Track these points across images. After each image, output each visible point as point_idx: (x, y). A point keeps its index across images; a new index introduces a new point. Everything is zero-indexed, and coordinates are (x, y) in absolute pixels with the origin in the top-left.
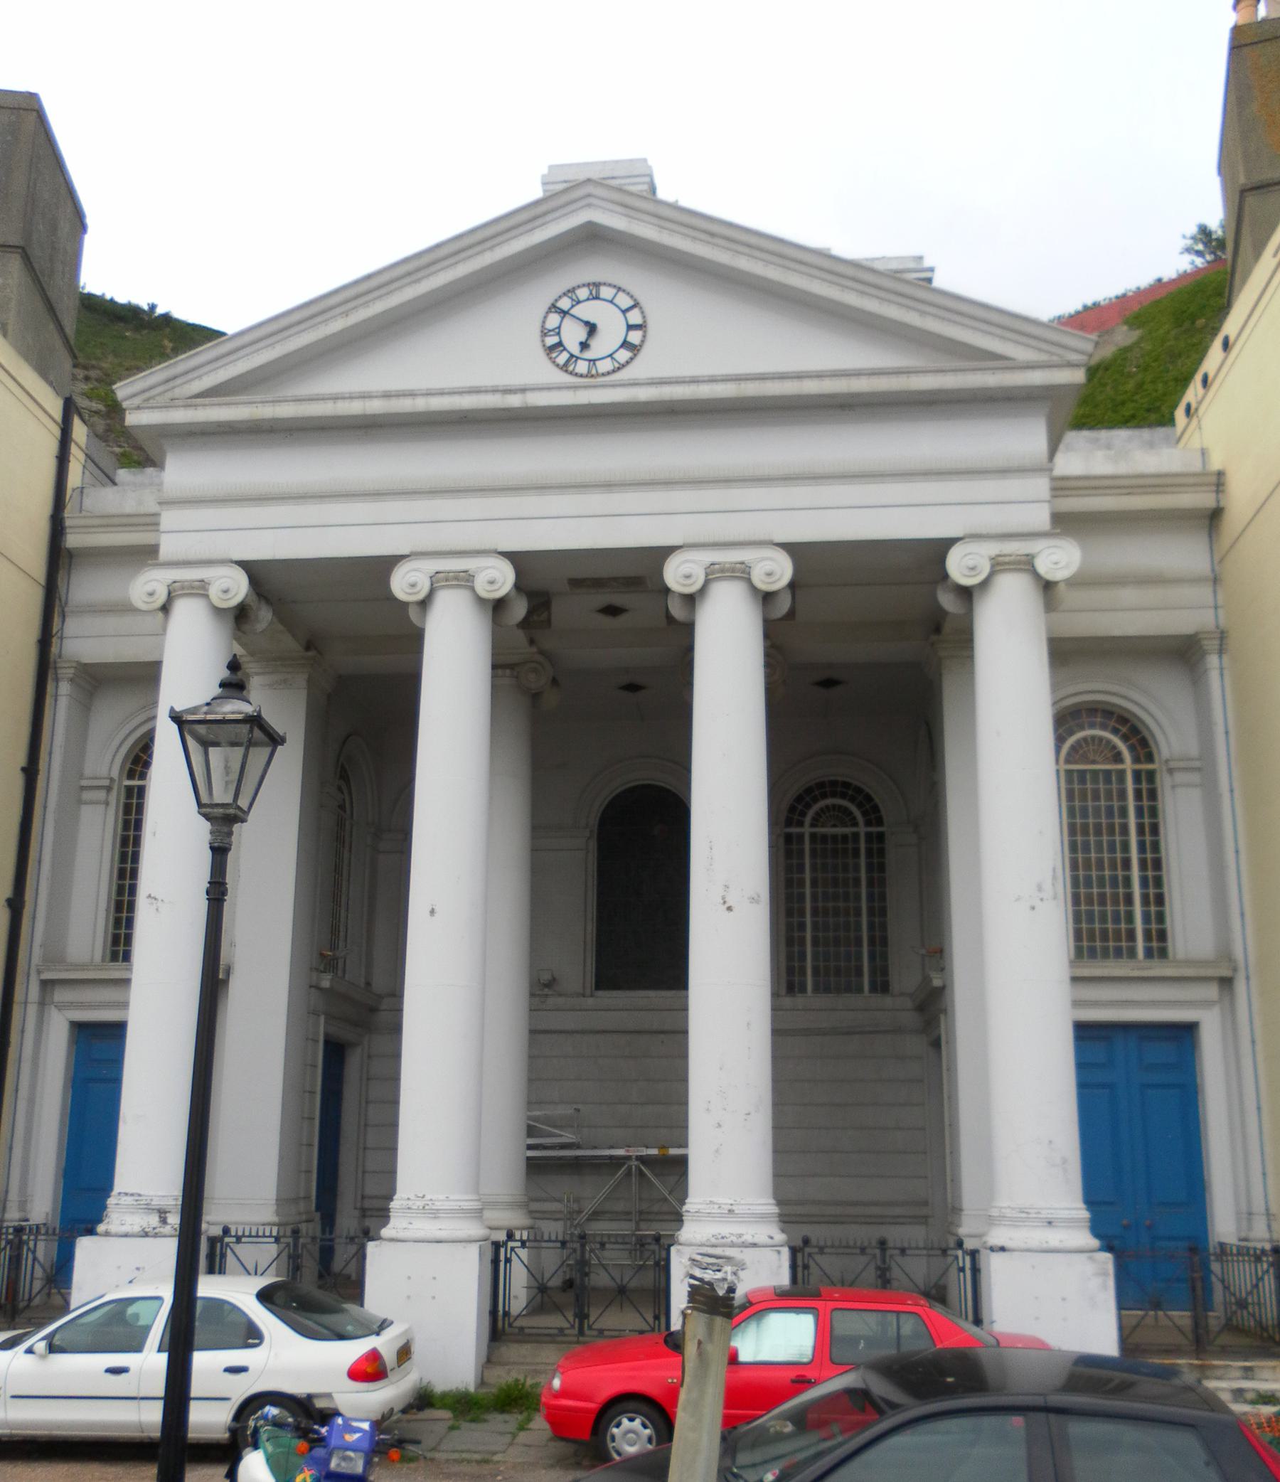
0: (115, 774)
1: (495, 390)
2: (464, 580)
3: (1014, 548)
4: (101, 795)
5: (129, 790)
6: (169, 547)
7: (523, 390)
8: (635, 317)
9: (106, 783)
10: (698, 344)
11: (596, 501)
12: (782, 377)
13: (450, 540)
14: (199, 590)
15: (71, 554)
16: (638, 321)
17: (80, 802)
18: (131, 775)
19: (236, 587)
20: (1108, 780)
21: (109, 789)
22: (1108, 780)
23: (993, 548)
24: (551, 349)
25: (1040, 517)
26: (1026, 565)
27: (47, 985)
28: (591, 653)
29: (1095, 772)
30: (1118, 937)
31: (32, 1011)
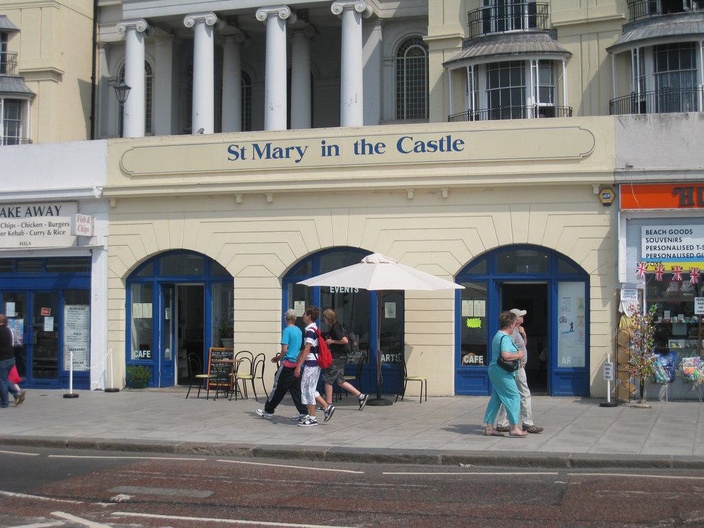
0: (118, 76)
14: (133, 28)
15: (100, 7)
17: (109, 85)
19: (143, 25)
20: (420, 61)
21: (117, 81)
22: (420, 61)
29: (415, 59)
30: (420, 112)
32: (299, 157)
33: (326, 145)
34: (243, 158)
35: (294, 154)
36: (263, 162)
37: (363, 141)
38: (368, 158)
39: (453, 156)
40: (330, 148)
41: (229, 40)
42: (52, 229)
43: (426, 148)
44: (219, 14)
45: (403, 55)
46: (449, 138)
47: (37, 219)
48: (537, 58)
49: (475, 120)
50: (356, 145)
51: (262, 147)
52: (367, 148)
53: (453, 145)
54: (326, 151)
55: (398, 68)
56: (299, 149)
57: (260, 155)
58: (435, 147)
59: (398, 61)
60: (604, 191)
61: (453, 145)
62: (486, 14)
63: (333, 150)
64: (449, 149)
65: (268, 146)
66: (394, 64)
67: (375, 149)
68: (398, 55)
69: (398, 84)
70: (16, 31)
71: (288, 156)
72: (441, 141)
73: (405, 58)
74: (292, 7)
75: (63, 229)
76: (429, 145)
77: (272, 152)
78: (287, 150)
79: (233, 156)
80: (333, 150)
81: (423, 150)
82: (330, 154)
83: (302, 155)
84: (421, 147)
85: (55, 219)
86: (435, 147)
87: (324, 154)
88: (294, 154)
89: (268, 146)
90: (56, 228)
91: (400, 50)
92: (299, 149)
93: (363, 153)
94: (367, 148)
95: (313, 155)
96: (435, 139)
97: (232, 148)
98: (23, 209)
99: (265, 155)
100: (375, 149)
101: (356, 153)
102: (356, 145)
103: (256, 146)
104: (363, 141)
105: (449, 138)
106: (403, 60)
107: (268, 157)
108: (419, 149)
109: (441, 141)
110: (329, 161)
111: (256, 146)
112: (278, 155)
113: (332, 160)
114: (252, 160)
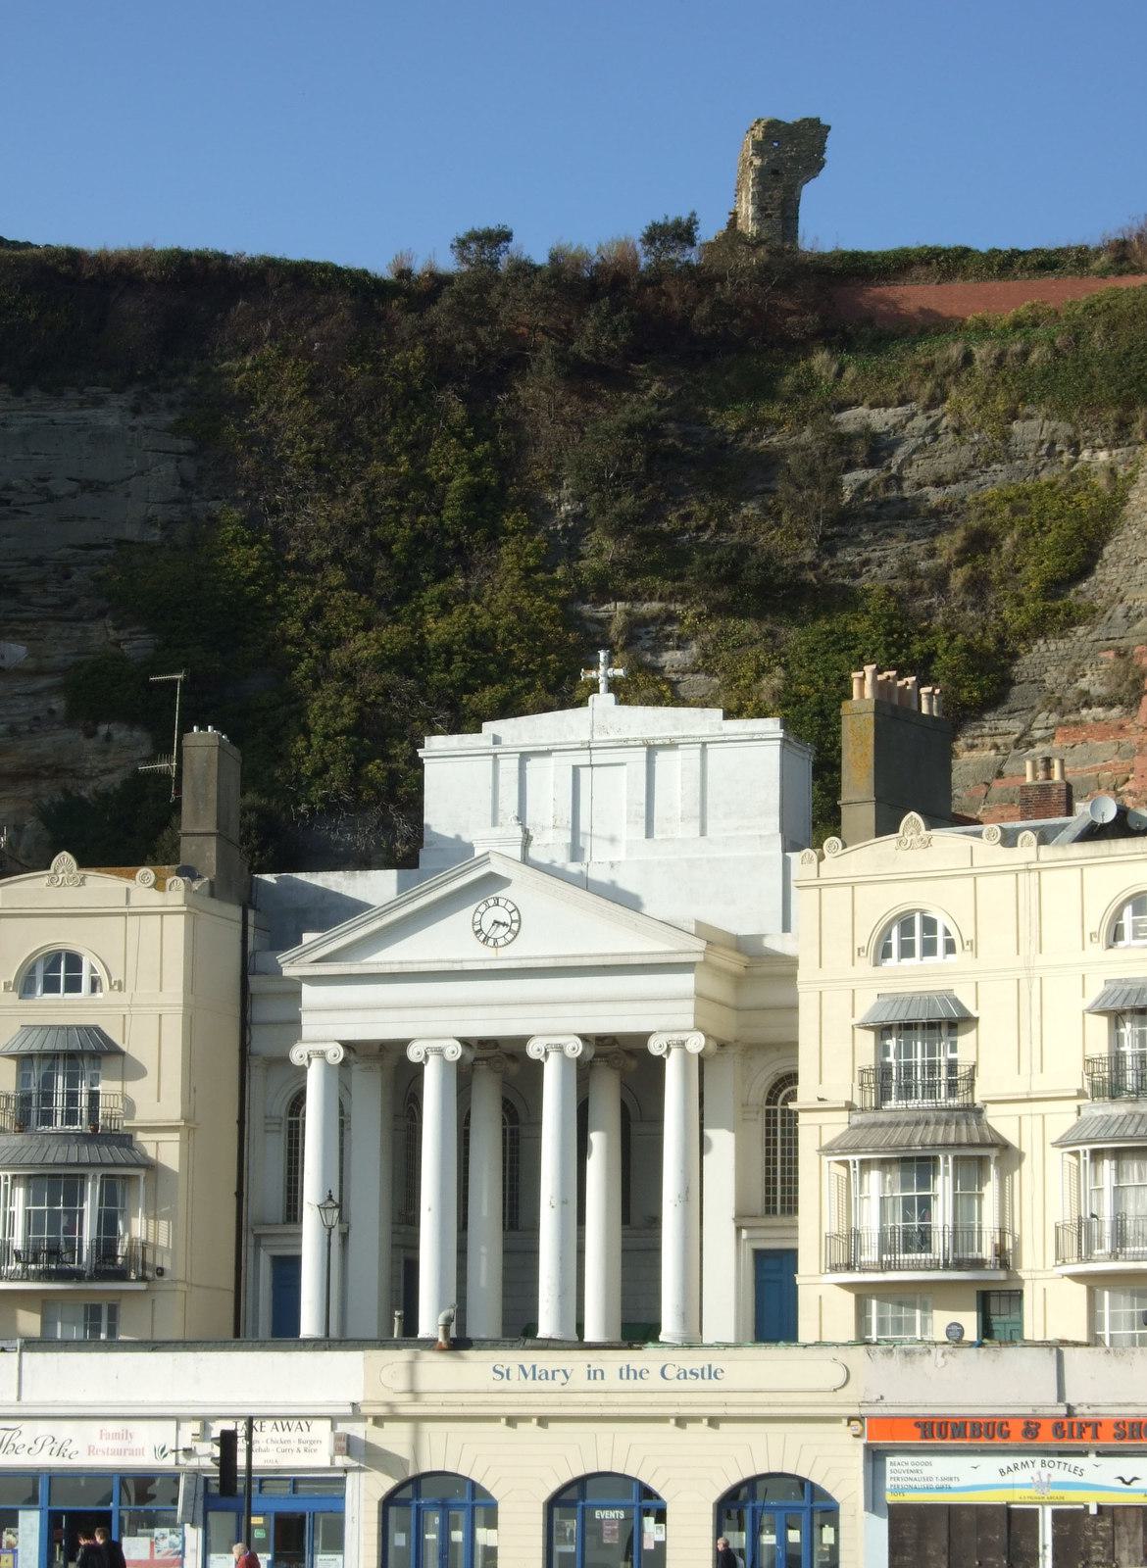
1: (448, 961)
3: (676, 1036)
4: (276, 1128)
5: (291, 1123)
6: (307, 1031)
7: (461, 961)
9: (278, 1121)
11: (497, 1011)
12: (574, 956)
13: (435, 1028)
16: (517, 918)
18: (291, 1115)
21: (280, 1124)
24: (477, 932)
25: (689, 1021)
26: (682, 1044)
27: (258, 1237)
31: (251, 1250)
32: (564, 1380)
33: (592, 1369)
34: (508, 1378)
35: (560, 1376)
36: (531, 1384)
37: (628, 1366)
38: (632, 1384)
39: (713, 1384)
40: (595, 1371)
41: (483, 1066)
42: (302, 1447)
43: (688, 1375)
44: (465, 1042)
45: (775, 1104)
46: (710, 1366)
47: (286, 1435)
50: (621, 1370)
51: (528, 1368)
52: (632, 1374)
53: (714, 1374)
54: (592, 1375)
55: (768, 1123)
56: (564, 1371)
57: (526, 1376)
58: (697, 1375)
59: (768, 1112)
60: (852, 1423)
61: (714, 1374)
63: (599, 1374)
64: (710, 1378)
65: (534, 1367)
66: (761, 1119)
68: (768, 1102)
69: (768, 1152)
71: (553, 1378)
72: (703, 1370)
73: (779, 1107)
74: (584, 1038)
75: (314, 1447)
76: (691, 1373)
77: (538, 1374)
78: (553, 1372)
79: (499, 1376)
80: (599, 1374)
81: (685, 1378)
82: (595, 1378)
83: (567, 1378)
84: (683, 1375)
85: (305, 1436)
86: (697, 1375)
87: (589, 1378)
88: (560, 1376)
89: (534, 1367)
90: (307, 1445)
91: (770, 1093)
92: (564, 1371)
93: (628, 1378)
94: (632, 1374)
95: (579, 1380)
96: (697, 1366)
97: (498, 1368)
99: (530, 1376)
100: (639, 1375)
101: (621, 1377)
102: (621, 1370)
103: (522, 1367)
104: (628, 1366)
105: (710, 1366)
106: (775, 1111)
107: (534, 1378)
108: (682, 1376)
109: (703, 1370)
110: (592, 1385)
111: (522, 1367)
112: (543, 1377)
114: (516, 1382)
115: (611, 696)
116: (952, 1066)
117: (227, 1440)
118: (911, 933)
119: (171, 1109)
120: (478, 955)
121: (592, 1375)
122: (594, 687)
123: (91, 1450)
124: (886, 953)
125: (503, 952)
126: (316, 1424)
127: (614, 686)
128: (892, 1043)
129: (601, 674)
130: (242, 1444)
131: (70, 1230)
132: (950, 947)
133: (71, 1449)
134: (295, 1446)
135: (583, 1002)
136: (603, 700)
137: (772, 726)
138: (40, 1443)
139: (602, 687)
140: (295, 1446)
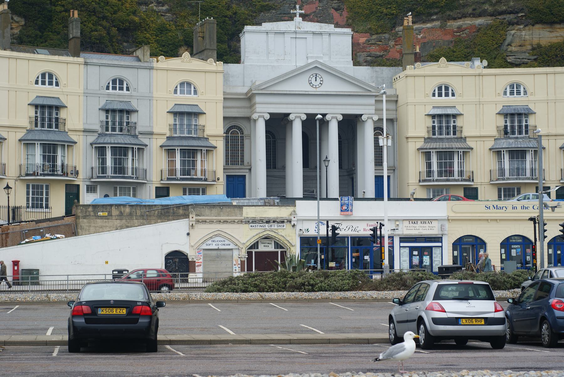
2: (300, 117)
3: (370, 116)
8: (321, 79)
10: (330, 85)
13: (298, 112)
23: (367, 116)
25: (373, 112)
28: (313, 126)
35: (504, 208)
36: (496, 210)
38: (525, 210)
48: (462, 151)
49: (42, 84)
51: (495, 206)
54: (513, 208)
62: (434, 127)
67: (527, 208)
70: (205, 113)
85: (430, 225)
88: (504, 208)
95: (510, 209)
98: (419, 222)
100: (527, 208)
113: (515, 211)
115: (301, 18)
116: (455, 127)
117: (334, 228)
118: (443, 90)
119: (220, 130)
120: (309, 89)
121: (513, 208)
122: (295, 15)
123: (364, 230)
124: (434, 95)
125: (318, 90)
126: (433, 222)
127: (301, 15)
128: (436, 120)
129: (298, 11)
130: (378, 230)
131: (450, 167)
132: (453, 95)
133: (358, 229)
134: (427, 228)
135: (287, 104)
136: (298, 19)
137: (348, 30)
138: (348, 227)
139: (298, 16)
140: (427, 228)
